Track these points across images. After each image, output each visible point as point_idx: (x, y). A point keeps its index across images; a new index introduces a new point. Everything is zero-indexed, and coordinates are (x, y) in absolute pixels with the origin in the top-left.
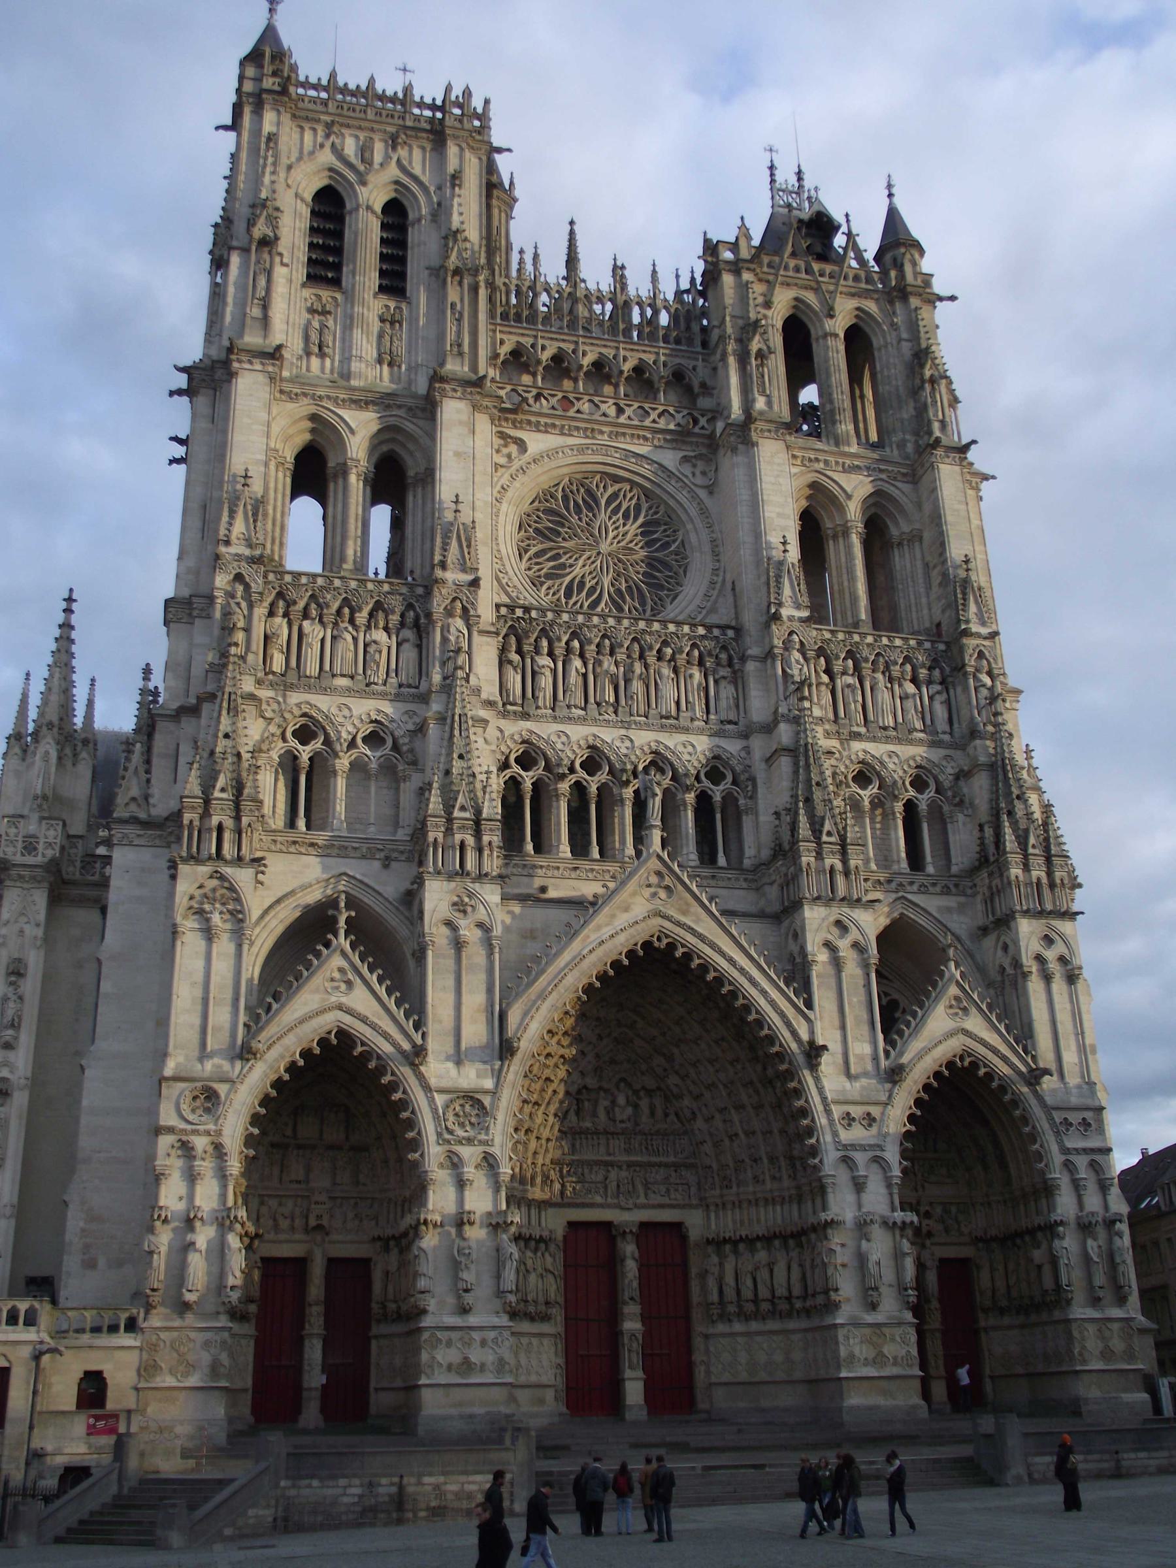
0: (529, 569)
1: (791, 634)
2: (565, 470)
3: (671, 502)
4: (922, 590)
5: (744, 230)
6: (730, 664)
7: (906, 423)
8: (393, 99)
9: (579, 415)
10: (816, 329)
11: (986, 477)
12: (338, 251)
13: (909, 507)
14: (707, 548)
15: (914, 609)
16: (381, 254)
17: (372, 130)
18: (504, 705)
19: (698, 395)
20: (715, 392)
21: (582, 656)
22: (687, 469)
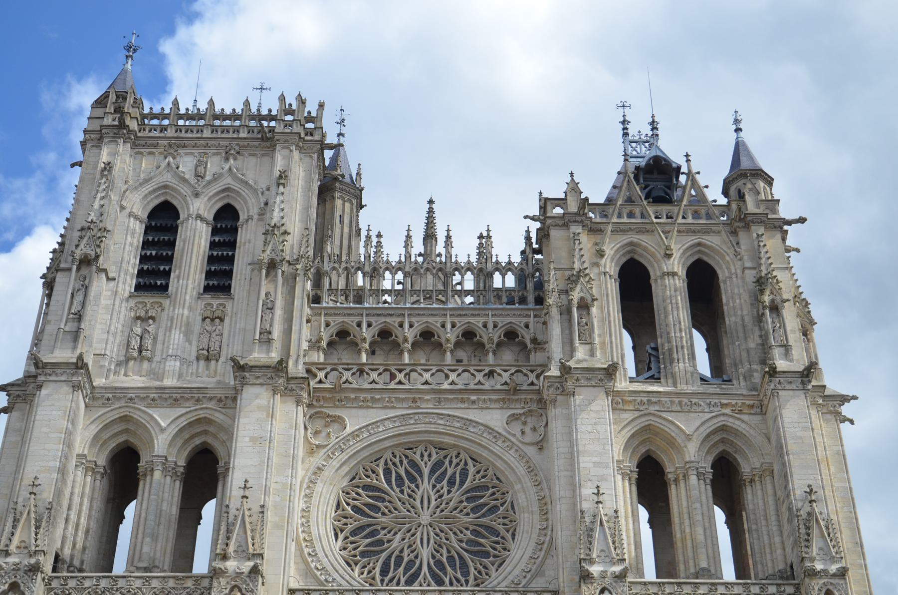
0: (345, 549)
2: (387, 444)
3: (499, 464)
4: (775, 528)
5: (574, 187)
7: (753, 353)
8: (234, 116)
9: (401, 386)
10: (654, 271)
11: (844, 399)
12: (169, 260)
13: (757, 439)
14: (536, 508)
15: (768, 550)
16: (209, 257)
17: (207, 146)
19: (530, 351)
20: (547, 345)
22: (516, 428)
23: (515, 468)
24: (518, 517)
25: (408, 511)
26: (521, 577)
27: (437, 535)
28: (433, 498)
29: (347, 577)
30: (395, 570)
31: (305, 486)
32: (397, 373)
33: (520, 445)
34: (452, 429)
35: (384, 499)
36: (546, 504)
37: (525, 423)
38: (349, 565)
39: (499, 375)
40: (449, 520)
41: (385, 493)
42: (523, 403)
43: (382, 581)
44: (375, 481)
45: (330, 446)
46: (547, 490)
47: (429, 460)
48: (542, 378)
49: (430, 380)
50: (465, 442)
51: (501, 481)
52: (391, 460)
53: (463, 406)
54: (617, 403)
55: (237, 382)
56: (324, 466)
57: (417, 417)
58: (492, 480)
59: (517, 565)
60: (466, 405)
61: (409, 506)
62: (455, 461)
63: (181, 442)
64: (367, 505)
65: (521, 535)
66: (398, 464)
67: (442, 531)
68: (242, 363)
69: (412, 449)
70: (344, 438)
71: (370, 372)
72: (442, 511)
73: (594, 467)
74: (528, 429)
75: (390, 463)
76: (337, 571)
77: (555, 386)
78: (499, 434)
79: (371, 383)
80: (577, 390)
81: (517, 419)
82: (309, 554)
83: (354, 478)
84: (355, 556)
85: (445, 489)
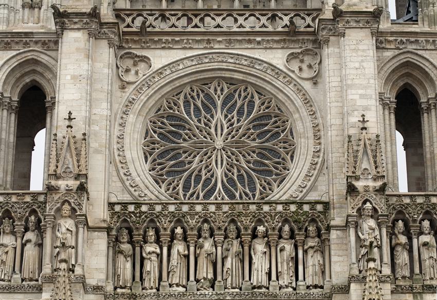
0: (154, 169)
1: (365, 202)
2: (186, 80)
3: (280, 96)
6: (319, 236)
9: (196, 30)
18: (115, 288)
21: (185, 238)
22: (295, 65)
23: (293, 100)
25: (205, 137)
27: (229, 157)
28: (225, 126)
29: (156, 193)
31: (118, 116)
32: (193, 17)
34: (241, 66)
35: (185, 127)
36: (319, 131)
37: (302, 61)
38: (157, 183)
39: (281, 18)
40: (239, 144)
42: (300, 43)
46: (320, 119)
47: (222, 94)
48: (317, 21)
49: (221, 23)
50: (252, 78)
51: (282, 112)
52: (190, 94)
53: (250, 46)
54: (381, 42)
55: (57, 27)
56: (133, 99)
57: (210, 56)
58: (274, 110)
59: (295, 182)
60: (252, 46)
61: (206, 134)
62: (243, 94)
63: (14, 80)
64: (170, 132)
65: (298, 156)
66: (196, 97)
67: (233, 154)
68: (61, 10)
69: (207, 84)
70: (150, 75)
71: (170, 17)
72: (233, 137)
73: (360, 98)
74: (304, 67)
75: (189, 97)
77: (329, 28)
79: (171, 27)
80: (347, 31)
81: (295, 58)
82: (125, 174)
83: (159, 110)
84: (162, 175)
85: (235, 119)
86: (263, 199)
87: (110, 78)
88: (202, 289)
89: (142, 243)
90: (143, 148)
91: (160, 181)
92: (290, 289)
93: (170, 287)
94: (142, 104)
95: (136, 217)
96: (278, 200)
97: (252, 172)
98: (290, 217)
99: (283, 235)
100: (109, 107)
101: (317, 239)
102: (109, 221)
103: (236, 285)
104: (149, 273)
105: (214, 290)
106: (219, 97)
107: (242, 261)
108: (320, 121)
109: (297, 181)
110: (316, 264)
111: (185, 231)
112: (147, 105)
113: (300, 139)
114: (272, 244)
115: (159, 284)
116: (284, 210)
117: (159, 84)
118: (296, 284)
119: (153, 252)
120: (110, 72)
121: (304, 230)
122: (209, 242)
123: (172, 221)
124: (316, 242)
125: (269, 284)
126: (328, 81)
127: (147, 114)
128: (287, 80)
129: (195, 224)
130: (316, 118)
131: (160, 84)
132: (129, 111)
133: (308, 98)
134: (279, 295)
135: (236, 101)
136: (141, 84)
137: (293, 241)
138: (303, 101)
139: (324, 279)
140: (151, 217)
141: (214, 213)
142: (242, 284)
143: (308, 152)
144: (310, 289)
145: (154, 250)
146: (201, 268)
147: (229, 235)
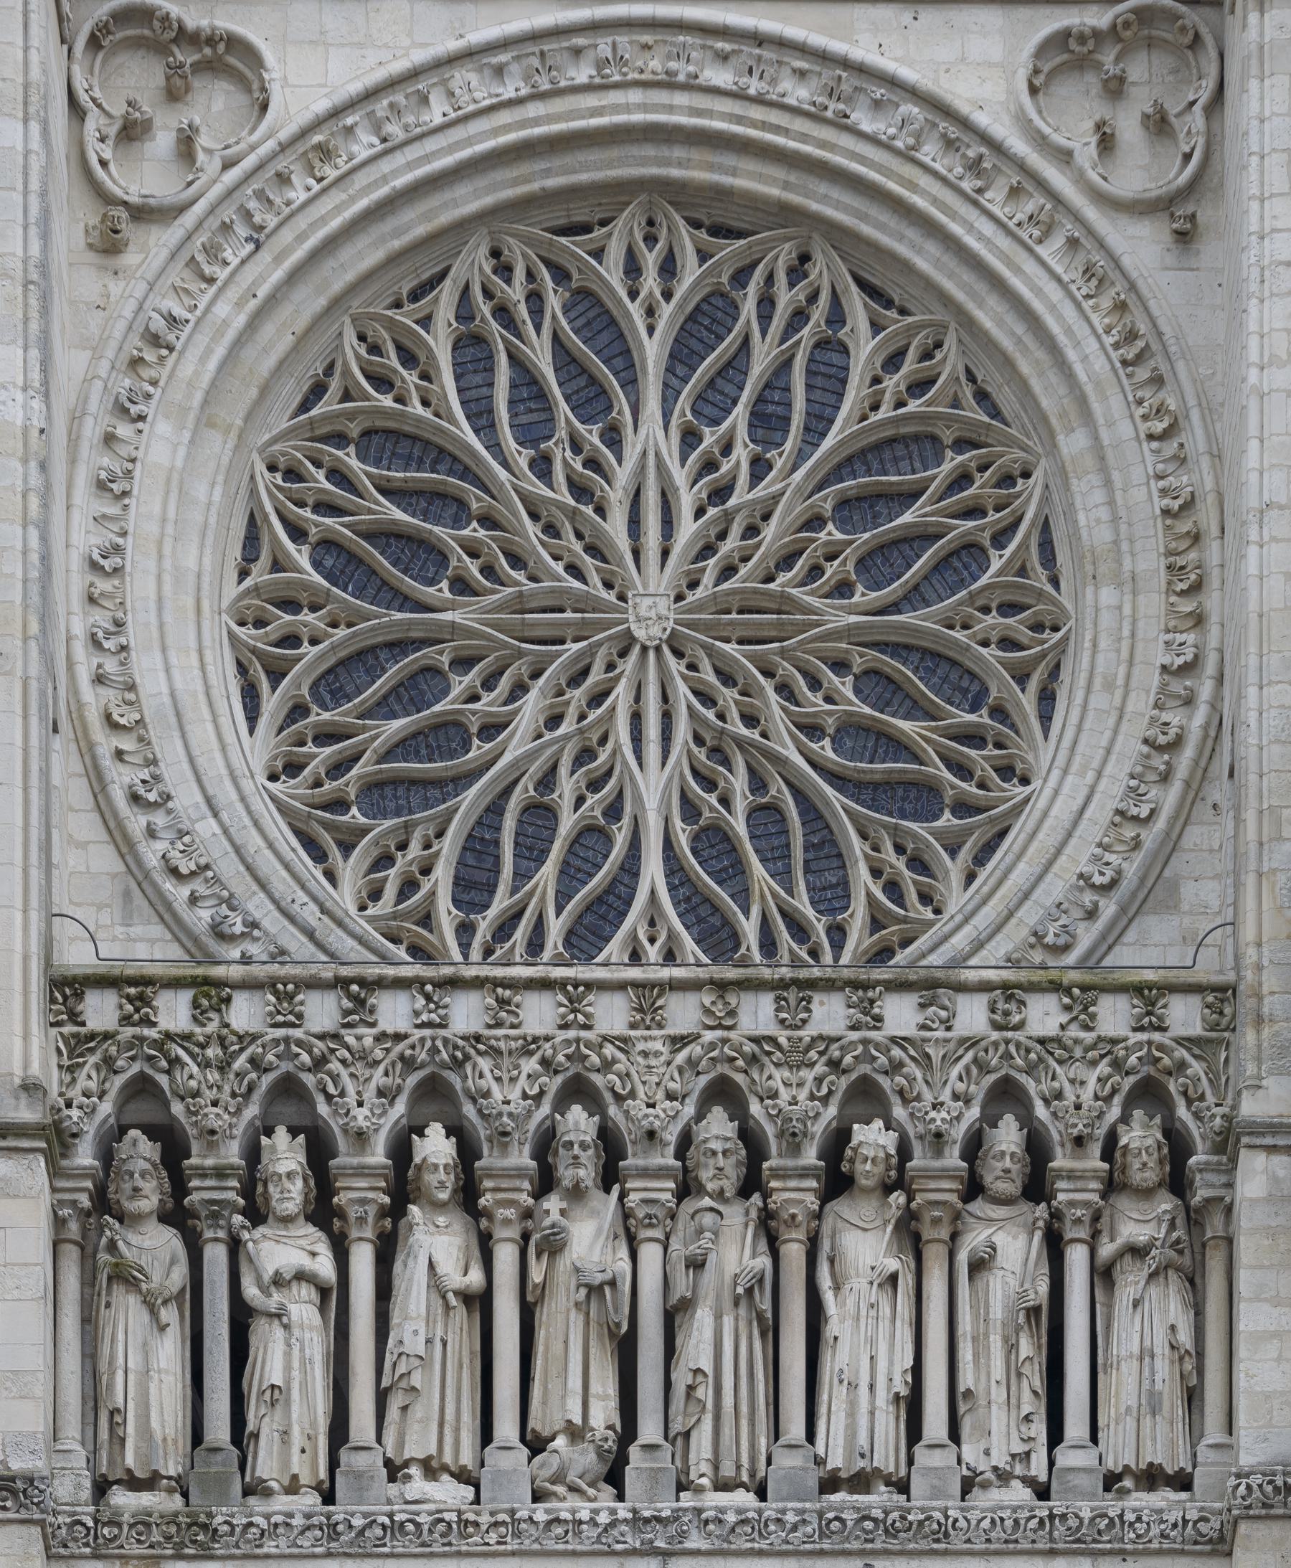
6: (1178, 1182)
18: (101, 1488)
23: (1062, 339)
24: (1069, 606)
25: (575, 570)
26: (1078, 913)
27: (706, 698)
28: (686, 501)
29: (310, 914)
30: (521, 876)
31: (91, 431)
33: (1091, 213)
35: (462, 504)
36: (1196, 538)
37: (1115, 88)
41: (466, 473)
43: (465, 931)
44: (419, 410)
45: (199, 208)
46: (1205, 462)
47: (668, 295)
51: (996, 413)
52: (488, 294)
56: (172, 320)
57: (604, 47)
58: (956, 404)
59: (1059, 852)
61: (578, 547)
62: (785, 298)
64: (384, 535)
66: (523, 311)
67: (727, 679)
69: (586, 229)
70: (260, 167)
72: (728, 571)
74: (1129, 127)
75: (485, 309)
76: (263, 886)
78: (996, 147)
81: (1082, 64)
82: (135, 798)
83: (318, 390)
85: (742, 454)
86: (883, 954)
87: (35, 185)
88: (560, 1489)
89: (238, 1219)
90: (231, 635)
91: (327, 840)
92: (1019, 1494)
93: (392, 1479)
94: (220, 351)
95: (205, 1064)
96: (959, 962)
97: (829, 791)
98: (1030, 1070)
99: (988, 1179)
100: (36, 376)
101: (1166, 1204)
102: (54, 1089)
103: (739, 1467)
104: (276, 1395)
105: (620, 1497)
106: (650, 312)
107: (772, 1331)
108: (1201, 476)
109: (1069, 850)
110: (1158, 1351)
111: (467, 1152)
112: (249, 353)
113: (1089, 590)
114: (927, 1233)
115: (333, 1464)
116: (997, 1026)
117: (314, 226)
118: (1051, 1463)
119: (301, 1276)
120: (35, 144)
121: (1096, 1149)
122: (595, 1213)
123: (399, 1089)
124: (1159, 1220)
125: (910, 1462)
126: (1254, 228)
127: (247, 419)
128: (1030, 207)
129: (518, 1106)
130: (1184, 461)
131: (323, 220)
132: (148, 396)
133: (1143, 328)
134: (962, 1523)
135: (746, 341)
136: (214, 223)
137: (1041, 1210)
138: (1116, 346)
139: (1195, 1432)
140: (286, 1066)
141: (625, 1040)
142: (769, 1463)
143: (1136, 671)
144: (1124, 1492)
145: (304, 1261)
146: (553, 1371)
147: (705, 1175)
